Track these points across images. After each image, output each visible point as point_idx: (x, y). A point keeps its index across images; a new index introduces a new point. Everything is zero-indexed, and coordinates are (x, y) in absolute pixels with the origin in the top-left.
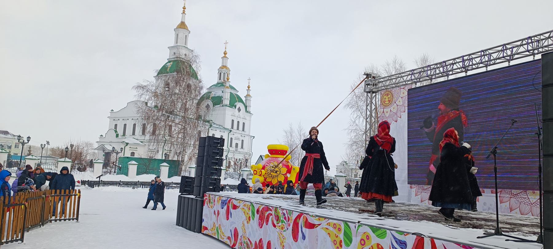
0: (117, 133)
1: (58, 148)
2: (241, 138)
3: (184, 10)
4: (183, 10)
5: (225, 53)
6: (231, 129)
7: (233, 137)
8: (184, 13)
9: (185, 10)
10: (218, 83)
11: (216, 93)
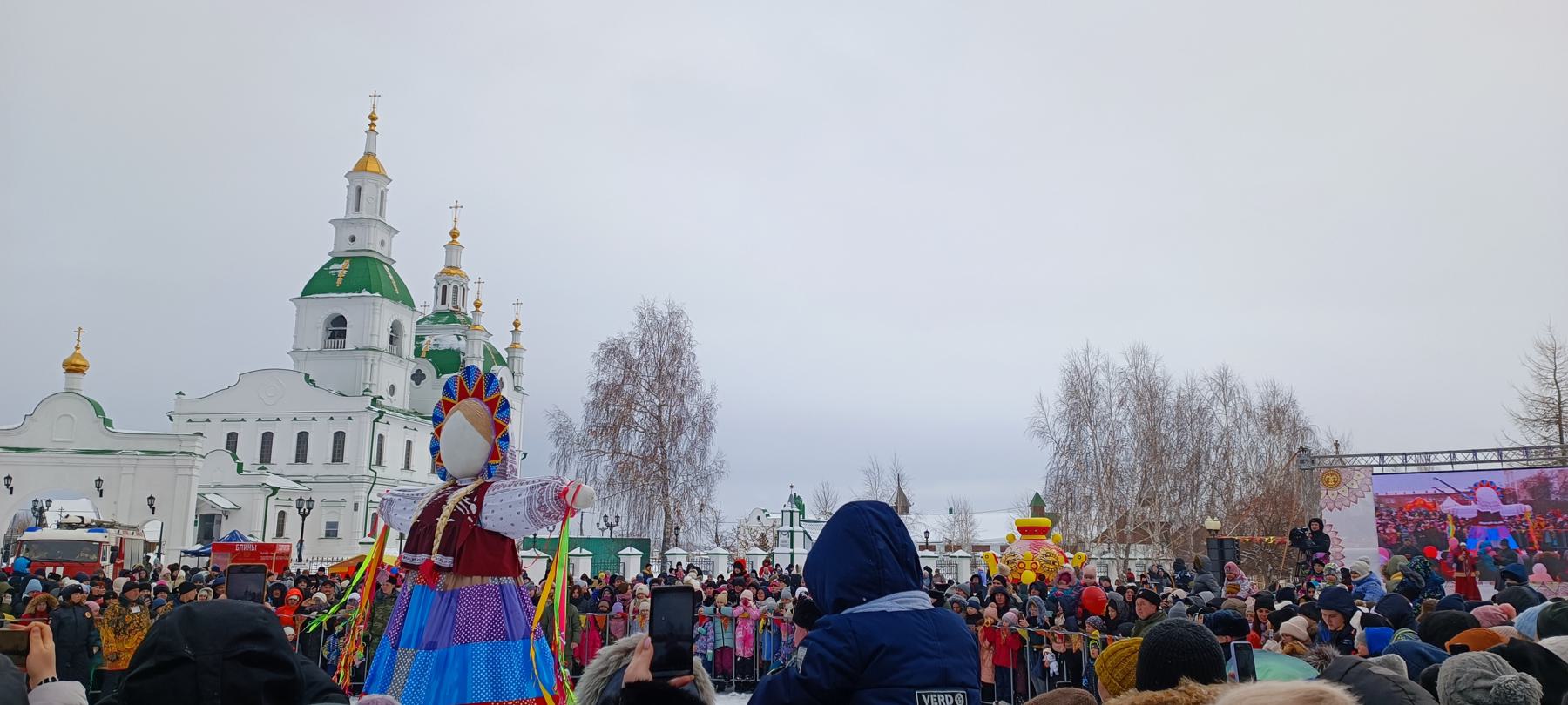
4: (370, 122)
5: (454, 235)
8: (373, 131)
9: (375, 122)
10: (438, 316)
11: (439, 339)
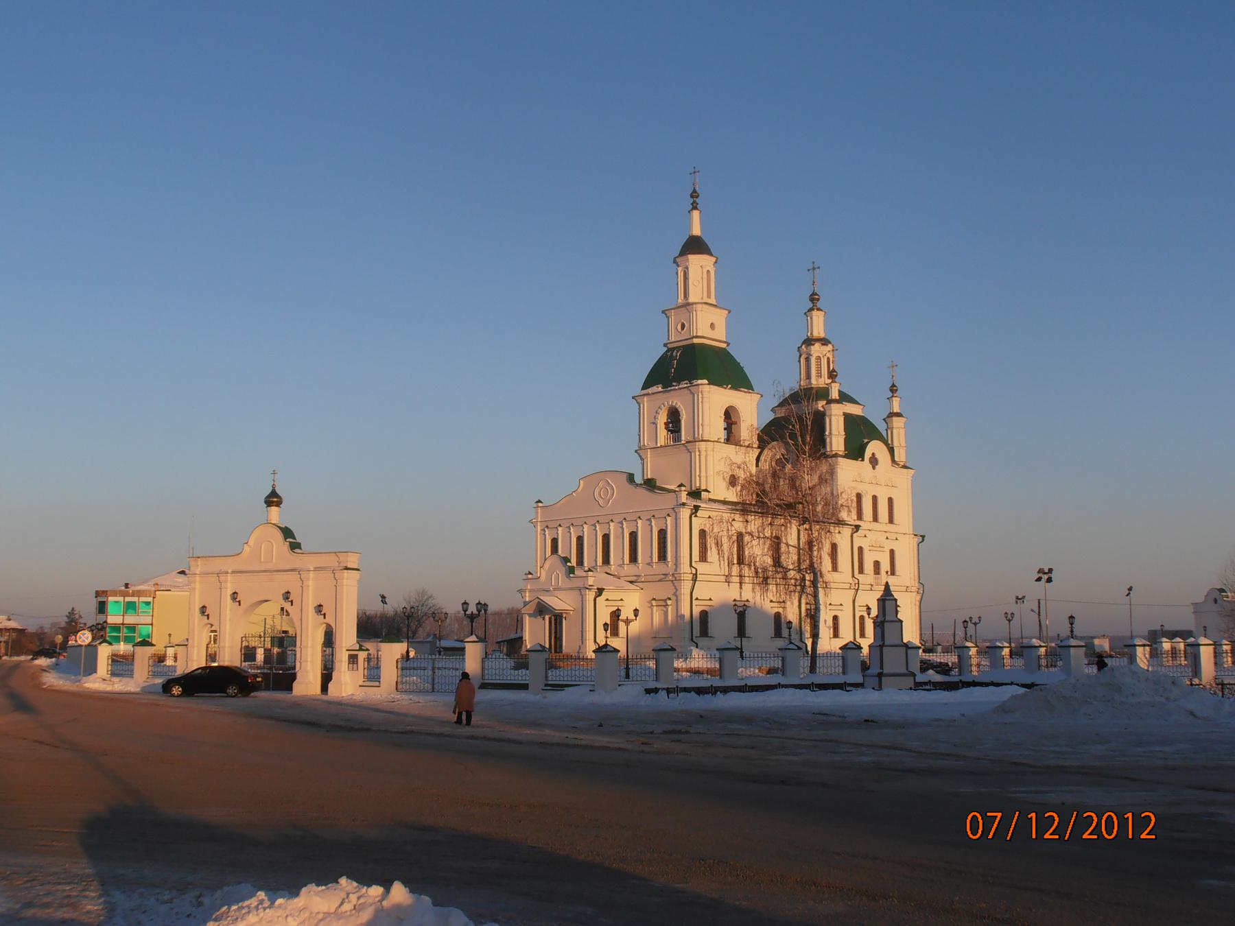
0: (569, 564)
1: (365, 613)
2: (889, 545)
3: (694, 202)
4: (692, 200)
6: (858, 523)
7: (865, 543)
